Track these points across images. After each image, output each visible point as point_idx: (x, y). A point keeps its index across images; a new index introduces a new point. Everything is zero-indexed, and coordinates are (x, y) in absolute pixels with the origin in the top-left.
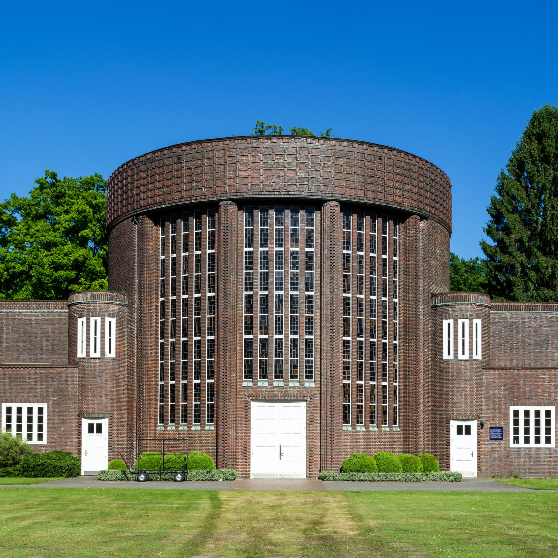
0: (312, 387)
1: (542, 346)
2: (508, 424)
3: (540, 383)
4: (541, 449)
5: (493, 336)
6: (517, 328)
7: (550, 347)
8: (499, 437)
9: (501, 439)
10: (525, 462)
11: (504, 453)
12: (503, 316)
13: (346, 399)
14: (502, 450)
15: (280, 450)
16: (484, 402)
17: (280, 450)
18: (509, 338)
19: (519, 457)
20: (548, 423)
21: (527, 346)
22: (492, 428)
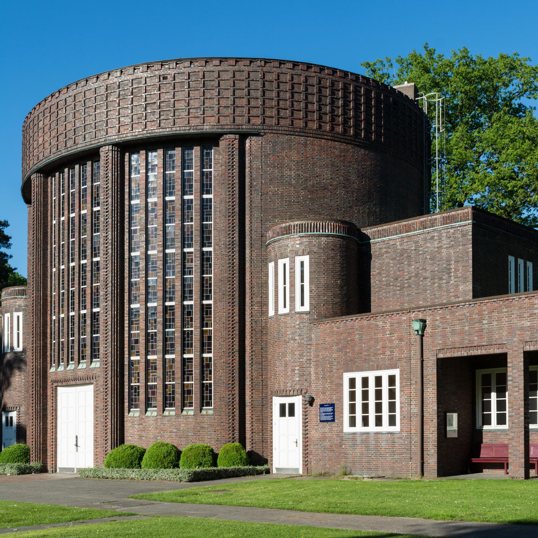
0: (97, 368)
1: (441, 279)
2: (341, 399)
3: (380, 336)
4: (381, 434)
5: (379, 274)
6: (409, 257)
7: (452, 278)
8: (329, 418)
9: (333, 420)
10: (362, 454)
11: (336, 441)
12: (391, 243)
13: (135, 379)
14: (334, 437)
15: (77, 441)
16: (312, 370)
17: (77, 441)
18: (398, 273)
19: (354, 445)
20: (392, 394)
21: (422, 281)
22: (322, 406)
